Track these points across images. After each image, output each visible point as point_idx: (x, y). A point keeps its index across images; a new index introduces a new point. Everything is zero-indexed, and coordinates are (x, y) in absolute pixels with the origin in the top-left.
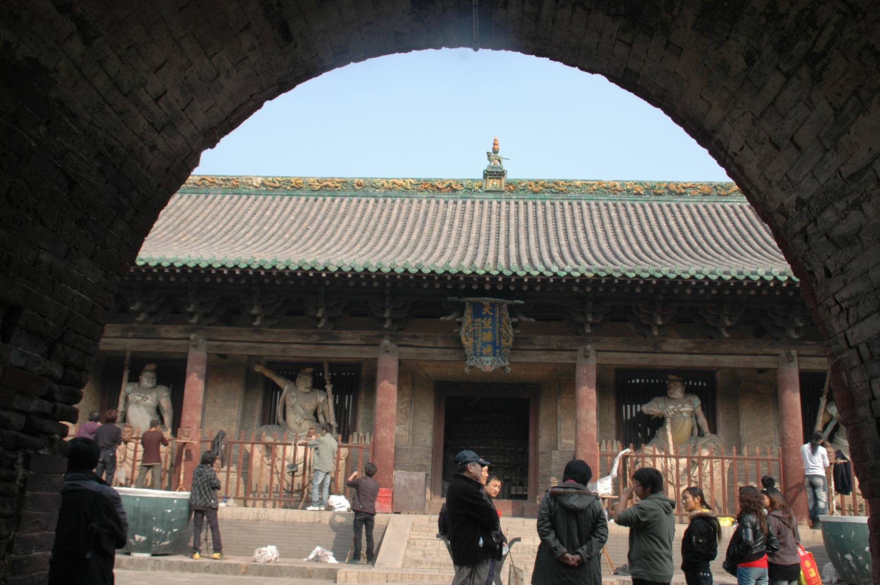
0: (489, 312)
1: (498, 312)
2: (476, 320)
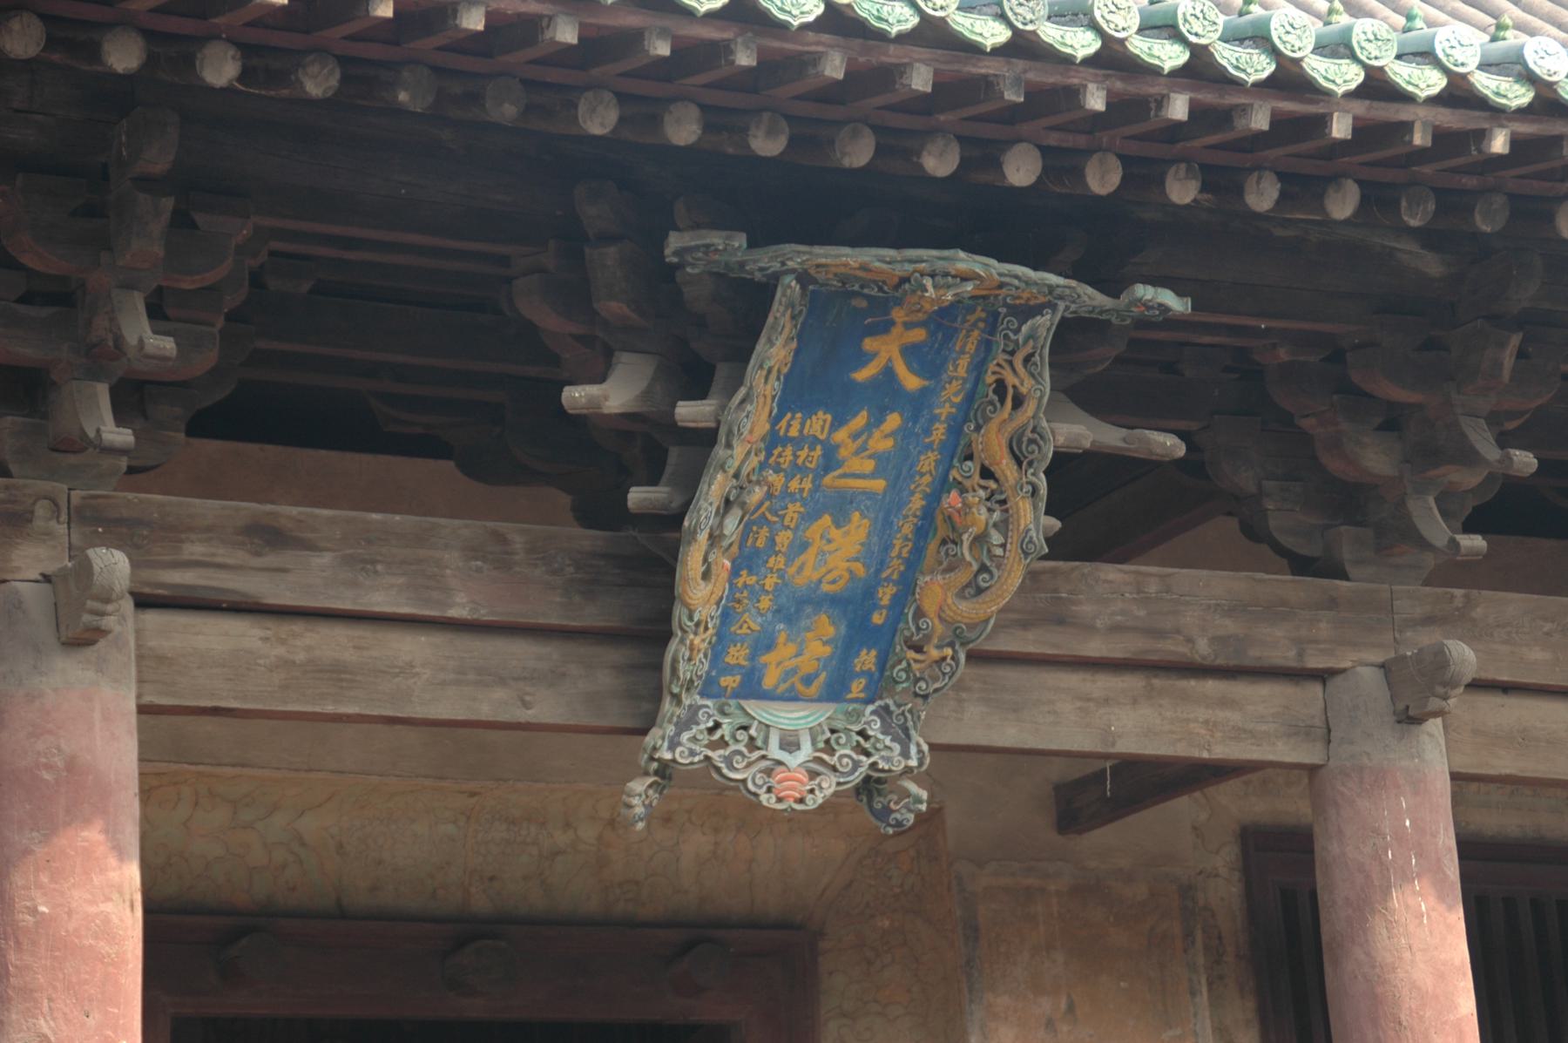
0: (901, 369)
1: (963, 366)
2: (793, 425)
